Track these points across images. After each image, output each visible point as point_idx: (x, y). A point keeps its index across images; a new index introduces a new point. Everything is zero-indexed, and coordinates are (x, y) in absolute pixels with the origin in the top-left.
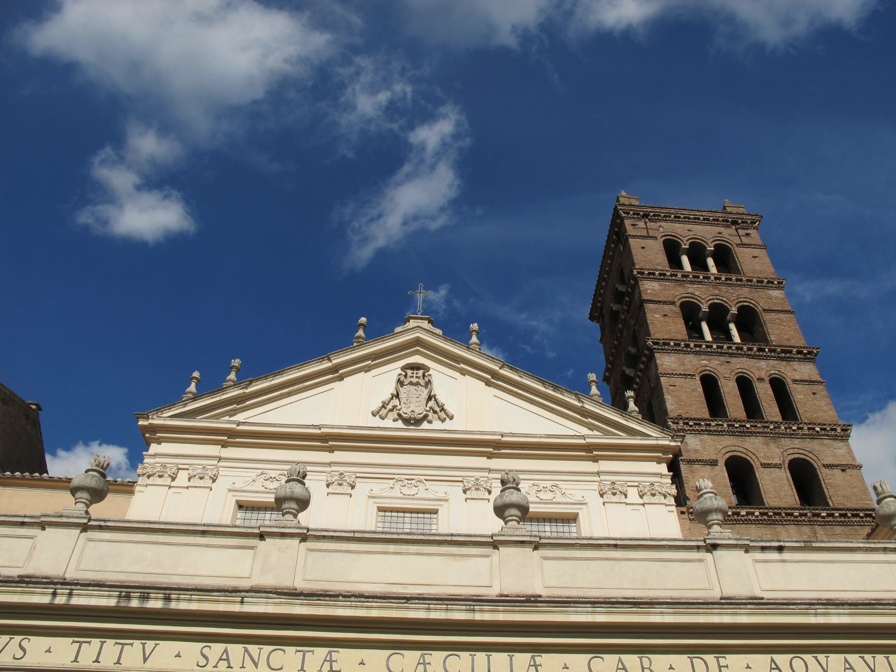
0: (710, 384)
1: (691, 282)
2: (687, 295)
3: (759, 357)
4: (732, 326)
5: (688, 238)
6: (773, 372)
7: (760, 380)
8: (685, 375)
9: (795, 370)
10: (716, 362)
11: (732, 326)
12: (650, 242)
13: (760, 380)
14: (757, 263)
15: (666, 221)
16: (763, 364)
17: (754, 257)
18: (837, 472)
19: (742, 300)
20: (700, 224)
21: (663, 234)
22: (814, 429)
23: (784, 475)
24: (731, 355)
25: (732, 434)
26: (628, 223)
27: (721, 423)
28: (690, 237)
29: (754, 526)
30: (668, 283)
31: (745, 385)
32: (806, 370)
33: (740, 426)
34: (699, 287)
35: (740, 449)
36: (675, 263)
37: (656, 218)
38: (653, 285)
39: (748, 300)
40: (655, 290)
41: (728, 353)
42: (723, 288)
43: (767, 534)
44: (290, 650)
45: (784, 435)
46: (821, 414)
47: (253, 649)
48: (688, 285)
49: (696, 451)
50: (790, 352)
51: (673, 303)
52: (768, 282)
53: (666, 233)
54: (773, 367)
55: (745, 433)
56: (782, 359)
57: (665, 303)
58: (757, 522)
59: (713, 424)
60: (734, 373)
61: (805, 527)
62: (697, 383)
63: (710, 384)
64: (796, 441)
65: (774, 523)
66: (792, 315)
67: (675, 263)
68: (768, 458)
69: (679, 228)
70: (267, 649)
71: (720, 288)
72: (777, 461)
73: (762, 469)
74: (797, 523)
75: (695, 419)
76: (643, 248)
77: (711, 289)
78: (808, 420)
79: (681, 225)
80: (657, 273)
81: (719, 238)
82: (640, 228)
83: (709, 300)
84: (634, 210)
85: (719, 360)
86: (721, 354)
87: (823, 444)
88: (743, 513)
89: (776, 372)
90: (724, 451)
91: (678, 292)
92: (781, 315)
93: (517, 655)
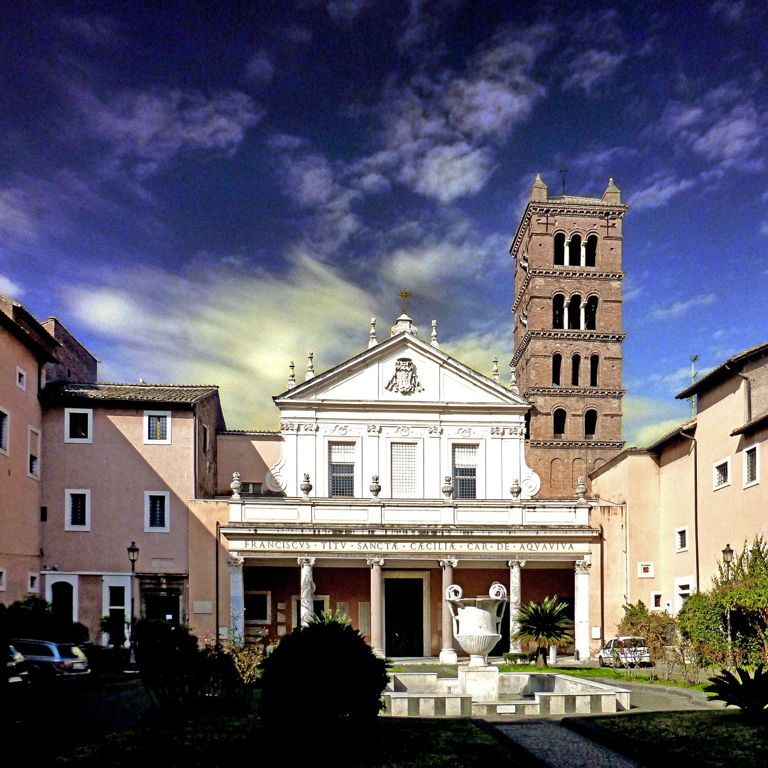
0: (557, 359)
1: (565, 278)
2: (560, 290)
3: (589, 340)
4: (583, 311)
5: (572, 232)
6: (595, 351)
7: (586, 358)
8: (544, 356)
9: (608, 349)
10: (565, 345)
11: (583, 311)
12: (546, 238)
13: (586, 358)
14: (612, 254)
15: (560, 214)
16: (591, 345)
17: (612, 249)
18: (609, 418)
19: (592, 292)
20: (583, 216)
21: (556, 229)
22: (604, 392)
23: (582, 420)
24: (574, 340)
25: (561, 396)
26: (535, 218)
27: (556, 390)
28: (574, 231)
29: (559, 450)
30: (550, 279)
31: (576, 359)
32: (614, 349)
33: (566, 391)
34: (567, 282)
35: (563, 405)
36: (559, 260)
37: (555, 212)
38: (541, 281)
39: (596, 292)
40: (541, 287)
41: (572, 339)
42: (584, 282)
43: (563, 454)
44: (384, 543)
45: (587, 396)
46: (612, 381)
47: (373, 544)
48: (562, 280)
49: (541, 406)
50: (608, 337)
51: (550, 298)
52: (613, 276)
53: (558, 229)
54: (597, 347)
55: (567, 396)
56: (604, 341)
57: (545, 298)
58: (562, 448)
59: (552, 390)
60: (572, 353)
61: (582, 450)
62: (550, 361)
63: (557, 359)
64: (593, 399)
65: (568, 448)
66: (620, 304)
67: (559, 260)
68: (575, 410)
69: (569, 221)
70: (377, 544)
71: (581, 282)
72: (580, 413)
73: (571, 417)
74: (580, 448)
75: (543, 388)
76: (540, 245)
77: (576, 283)
78: (605, 385)
79: (571, 218)
80: (544, 272)
81: (593, 231)
82: (542, 223)
83: (573, 293)
84: (540, 207)
85: (566, 343)
86: (569, 339)
87: (607, 401)
88: (555, 443)
89: (597, 351)
90: (555, 406)
91: (554, 288)
92: (614, 305)
93: (447, 544)
